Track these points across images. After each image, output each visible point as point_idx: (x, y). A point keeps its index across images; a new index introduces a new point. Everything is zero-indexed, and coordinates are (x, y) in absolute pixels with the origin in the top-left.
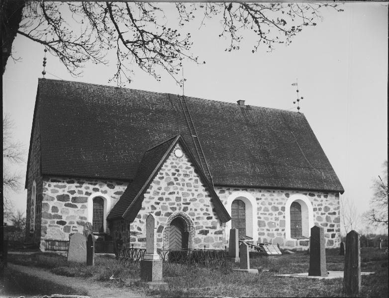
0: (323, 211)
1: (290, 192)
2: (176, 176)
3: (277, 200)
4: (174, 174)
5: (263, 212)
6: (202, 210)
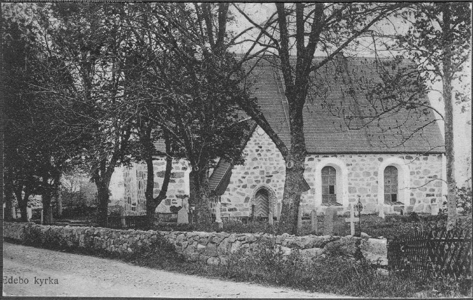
1: (383, 156)
2: (259, 152)
3: (369, 165)
4: (257, 151)
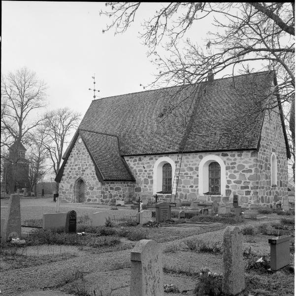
1: (203, 154)
3: (192, 162)
6: (91, 174)
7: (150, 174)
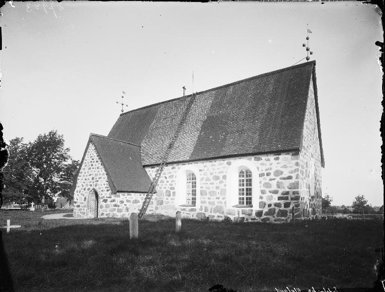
0: (272, 176)
1: (232, 160)
3: (218, 169)
5: (205, 182)
7: (172, 185)
